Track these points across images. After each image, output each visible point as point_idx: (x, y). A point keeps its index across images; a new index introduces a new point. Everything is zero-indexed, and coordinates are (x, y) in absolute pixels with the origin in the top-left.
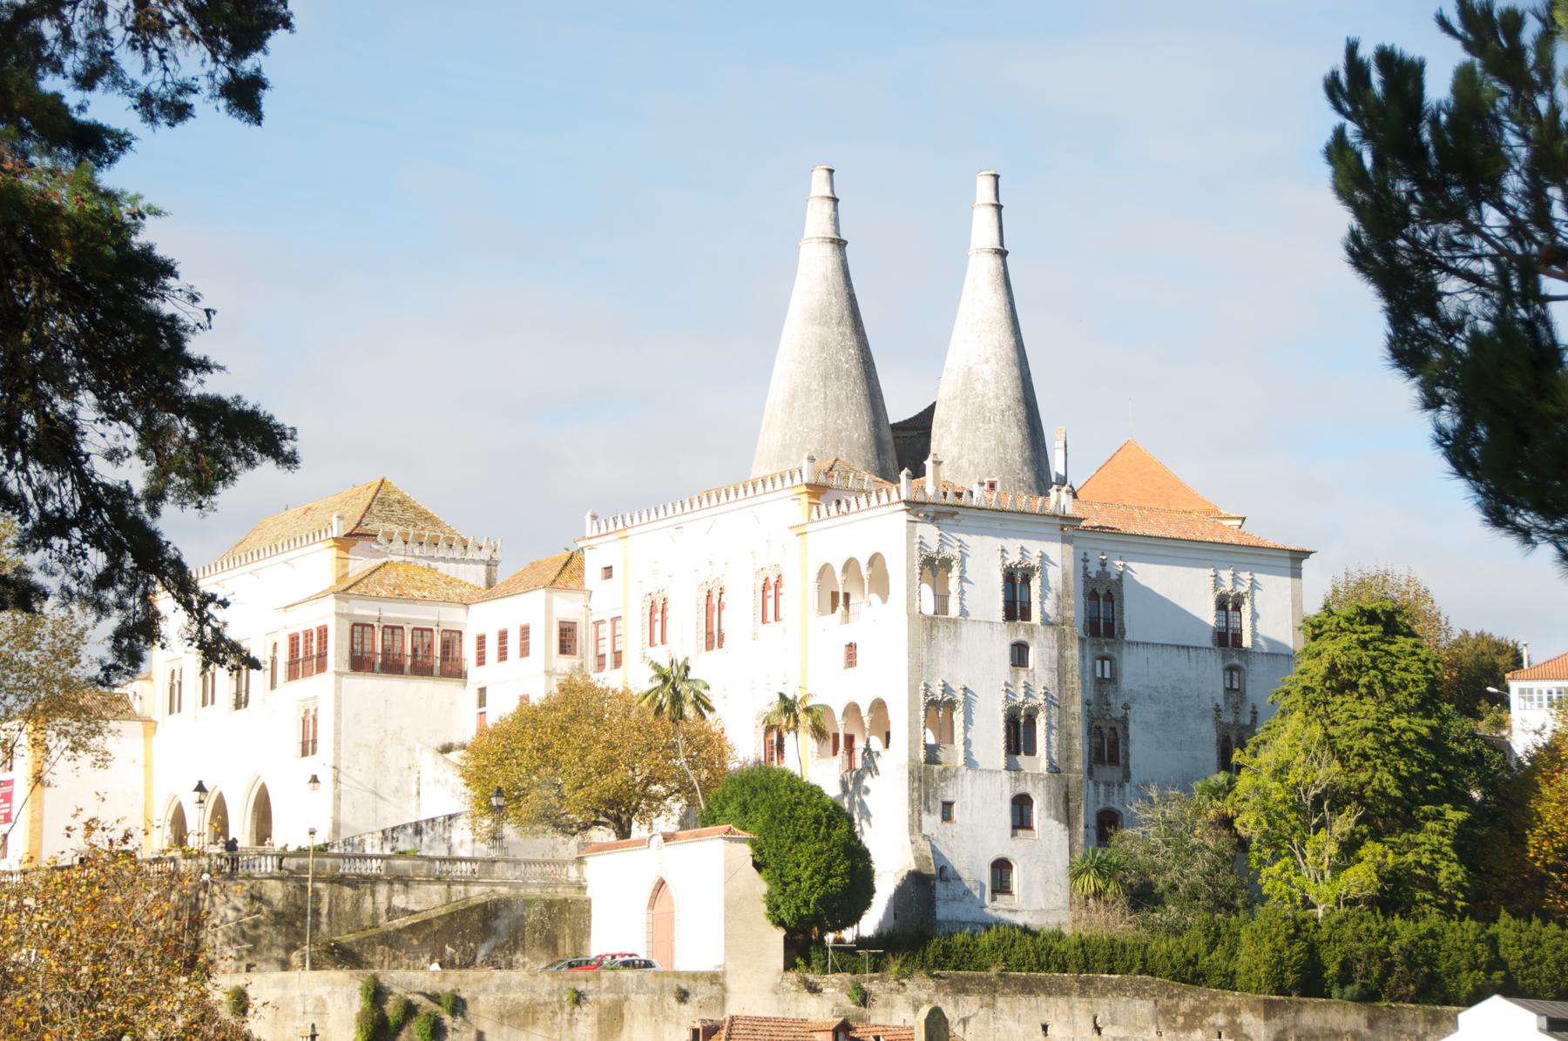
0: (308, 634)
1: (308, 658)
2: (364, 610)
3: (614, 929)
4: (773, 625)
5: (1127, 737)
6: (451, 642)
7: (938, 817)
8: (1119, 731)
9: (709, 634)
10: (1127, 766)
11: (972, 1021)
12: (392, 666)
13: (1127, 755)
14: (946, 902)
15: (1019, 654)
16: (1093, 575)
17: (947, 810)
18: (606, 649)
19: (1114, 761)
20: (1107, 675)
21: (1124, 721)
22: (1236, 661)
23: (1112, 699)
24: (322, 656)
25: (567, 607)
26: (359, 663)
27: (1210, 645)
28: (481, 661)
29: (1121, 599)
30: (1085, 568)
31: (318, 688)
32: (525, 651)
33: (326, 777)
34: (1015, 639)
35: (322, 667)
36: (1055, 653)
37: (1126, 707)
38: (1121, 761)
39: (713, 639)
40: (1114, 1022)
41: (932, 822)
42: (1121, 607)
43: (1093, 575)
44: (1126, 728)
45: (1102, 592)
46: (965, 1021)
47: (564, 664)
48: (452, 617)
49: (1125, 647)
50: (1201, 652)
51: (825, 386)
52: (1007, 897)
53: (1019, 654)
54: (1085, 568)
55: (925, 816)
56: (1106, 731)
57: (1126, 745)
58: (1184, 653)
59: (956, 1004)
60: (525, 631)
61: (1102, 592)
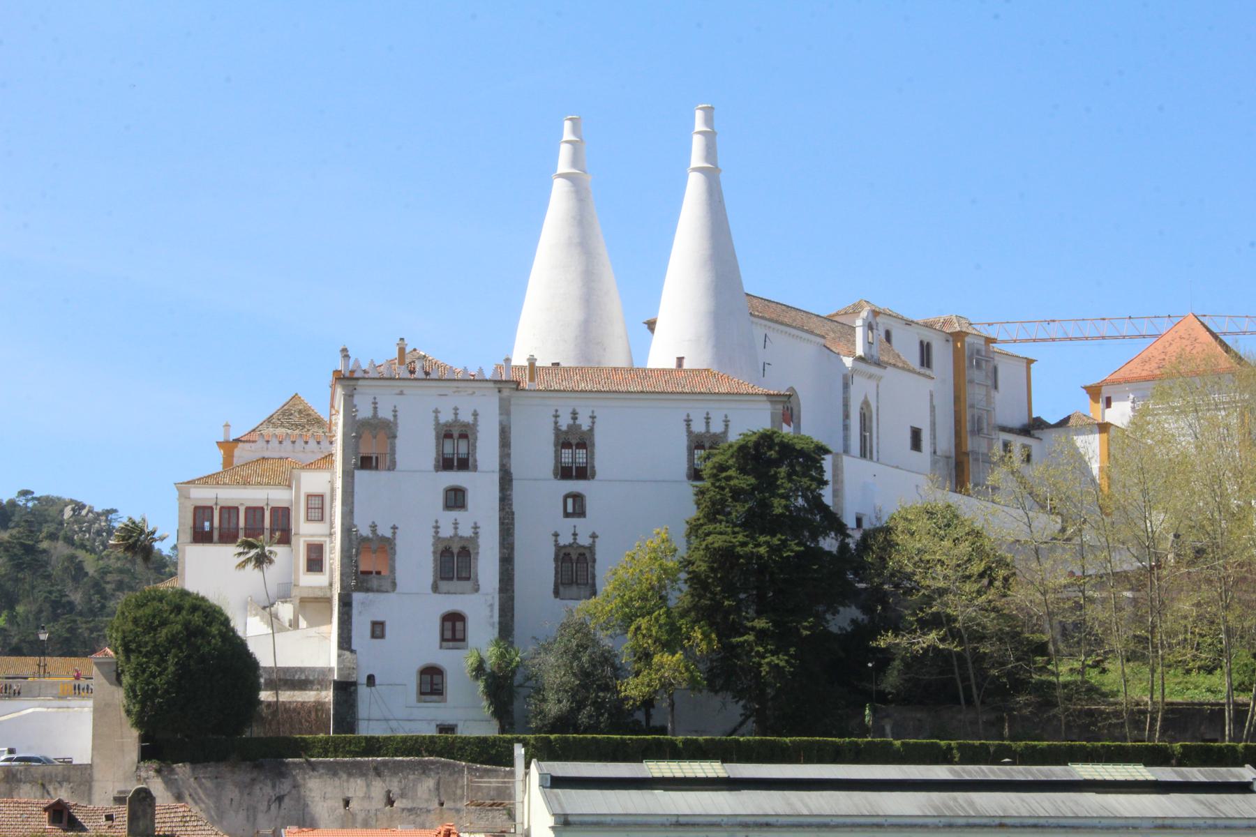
5: (594, 561)
8: (588, 555)
10: (594, 585)
11: (286, 800)
13: (594, 577)
15: (455, 499)
16: (564, 428)
17: (378, 630)
21: (591, 549)
26: (201, 536)
29: (593, 445)
30: (556, 423)
37: (594, 536)
40: (403, 796)
42: (593, 453)
43: (564, 428)
46: (280, 799)
53: (455, 499)
54: (556, 423)
57: (593, 567)
59: (274, 787)
61: (574, 442)
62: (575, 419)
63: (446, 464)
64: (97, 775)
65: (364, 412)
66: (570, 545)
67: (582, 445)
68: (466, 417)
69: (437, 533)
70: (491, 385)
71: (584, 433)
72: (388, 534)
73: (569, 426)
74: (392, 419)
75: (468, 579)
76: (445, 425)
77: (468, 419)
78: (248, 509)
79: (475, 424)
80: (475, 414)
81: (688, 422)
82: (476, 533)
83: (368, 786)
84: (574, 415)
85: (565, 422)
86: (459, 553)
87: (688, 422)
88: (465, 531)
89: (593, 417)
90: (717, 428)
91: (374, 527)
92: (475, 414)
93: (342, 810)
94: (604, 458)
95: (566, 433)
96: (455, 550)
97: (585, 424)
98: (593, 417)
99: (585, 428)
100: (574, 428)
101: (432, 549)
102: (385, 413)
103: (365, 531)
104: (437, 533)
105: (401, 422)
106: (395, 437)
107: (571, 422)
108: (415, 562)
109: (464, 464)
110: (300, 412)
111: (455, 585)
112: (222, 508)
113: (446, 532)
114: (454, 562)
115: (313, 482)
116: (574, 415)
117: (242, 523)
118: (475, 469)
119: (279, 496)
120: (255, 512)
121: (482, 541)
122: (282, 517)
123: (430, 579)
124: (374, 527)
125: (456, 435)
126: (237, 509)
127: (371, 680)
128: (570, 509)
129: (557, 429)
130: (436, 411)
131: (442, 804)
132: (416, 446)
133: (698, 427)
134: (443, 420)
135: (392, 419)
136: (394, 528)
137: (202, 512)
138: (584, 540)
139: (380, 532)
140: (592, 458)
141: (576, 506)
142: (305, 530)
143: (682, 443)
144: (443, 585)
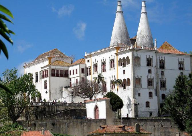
0: (45, 71)
1: (45, 74)
2: (53, 67)
3: (90, 114)
4: (113, 68)
6: (66, 72)
7: (138, 96)
9: (103, 70)
12: (57, 75)
17: (139, 95)
18: (89, 73)
19: (164, 87)
21: (165, 81)
22: (182, 72)
24: (47, 74)
25: (83, 66)
26: (53, 75)
28: (70, 75)
29: (165, 63)
31: (47, 79)
32: (77, 73)
33: (48, 92)
35: (47, 76)
39: (104, 70)
40: (164, 125)
41: (137, 96)
44: (166, 82)
45: (162, 62)
46: (142, 125)
47: (82, 75)
48: (66, 68)
52: (148, 107)
53: (150, 71)
56: (163, 83)
60: (77, 70)
61: (162, 62)
62: (162, 58)
63: (148, 65)
64: (107, 121)
65: (136, 55)
66: (162, 81)
68: (151, 57)
69: (147, 78)
70: (155, 51)
72: (140, 78)
75: (152, 86)
78: (61, 70)
80: (152, 57)
82: (153, 78)
83: (158, 123)
85: (161, 58)
88: (152, 78)
89: (165, 58)
91: (138, 76)
92: (152, 57)
93: (153, 128)
94: (167, 65)
96: (150, 81)
97: (163, 59)
98: (165, 58)
99: (164, 60)
100: (162, 59)
102: (139, 56)
103: (137, 77)
104: (147, 78)
105: (141, 57)
106: (140, 60)
108: (144, 83)
109: (151, 65)
111: (150, 87)
113: (149, 78)
114: (150, 83)
117: (60, 73)
118: (153, 66)
120: (62, 71)
121: (154, 80)
124: (138, 76)
125: (149, 60)
126: (59, 70)
127: (139, 103)
129: (159, 59)
130: (146, 56)
131: (171, 127)
132: (143, 62)
133: (180, 60)
137: (53, 70)
138: (164, 80)
141: (162, 73)
144: (149, 87)
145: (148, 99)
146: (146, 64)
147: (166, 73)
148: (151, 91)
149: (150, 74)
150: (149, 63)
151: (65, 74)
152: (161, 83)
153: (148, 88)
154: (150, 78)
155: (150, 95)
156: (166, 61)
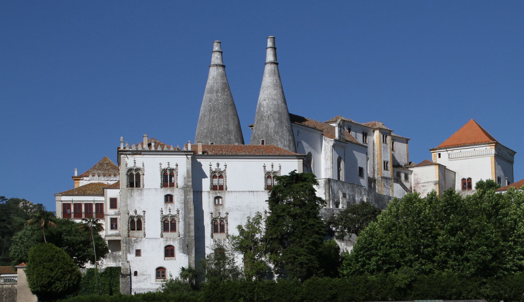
7: (134, 255)
14: (136, 283)
16: (214, 170)
17: (138, 253)
20: (221, 203)
21: (226, 218)
23: (221, 211)
27: (264, 190)
34: (166, 194)
36: (183, 197)
38: (226, 232)
44: (227, 221)
49: (227, 193)
50: (259, 193)
51: (210, 114)
53: (169, 199)
55: (128, 255)
58: (251, 194)
62: (218, 166)
65: (131, 165)
67: (221, 177)
71: (222, 172)
72: (142, 214)
73: (216, 169)
74: (142, 167)
76: (164, 169)
77: (174, 167)
78: (85, 204)
79: (177, 169)
80: (177, 165)
81: (265, 167)
84: (218, 165)
86: (171, 221)
87: (265, 167)
88: (174, 213)
90: (276, 169)
95: (215, 172)
99: (222, 170)
101: (160, 220)
102: (139, 165)
103: (132, 213)
107: (217, 167)
108: (152, 225)
109: (172, 185)
110: (107, 164)
112: (74, 204)
113: (166, 213)
114: (168, 225)
115: (111, 193)
116: (218, 165)
119: (99, 199)
120: (88, 206)
122: (100, 206)
123: (160, 232)
124: (136, 212)
127: (136, 273)
128: (217, 203)
133: (269, 169)
134: (163, 168)
135: (142, 167)
136: (144, 212)
137: (66, 206)
138: (223, 215)
139: (138, 214)
140: (226, 182)
142: (109, 212)
143: (263, 175)
145: (161, 261)
146: (158, 180)
147: (229, 200)
148: (171, 243)
149: (169, 205)
150: (167, 178)
151: (86, 213)
152: (214, 222)
153: (162, 236)
154: (168, 213)
155: (169, 252)
156: (228, 173)
